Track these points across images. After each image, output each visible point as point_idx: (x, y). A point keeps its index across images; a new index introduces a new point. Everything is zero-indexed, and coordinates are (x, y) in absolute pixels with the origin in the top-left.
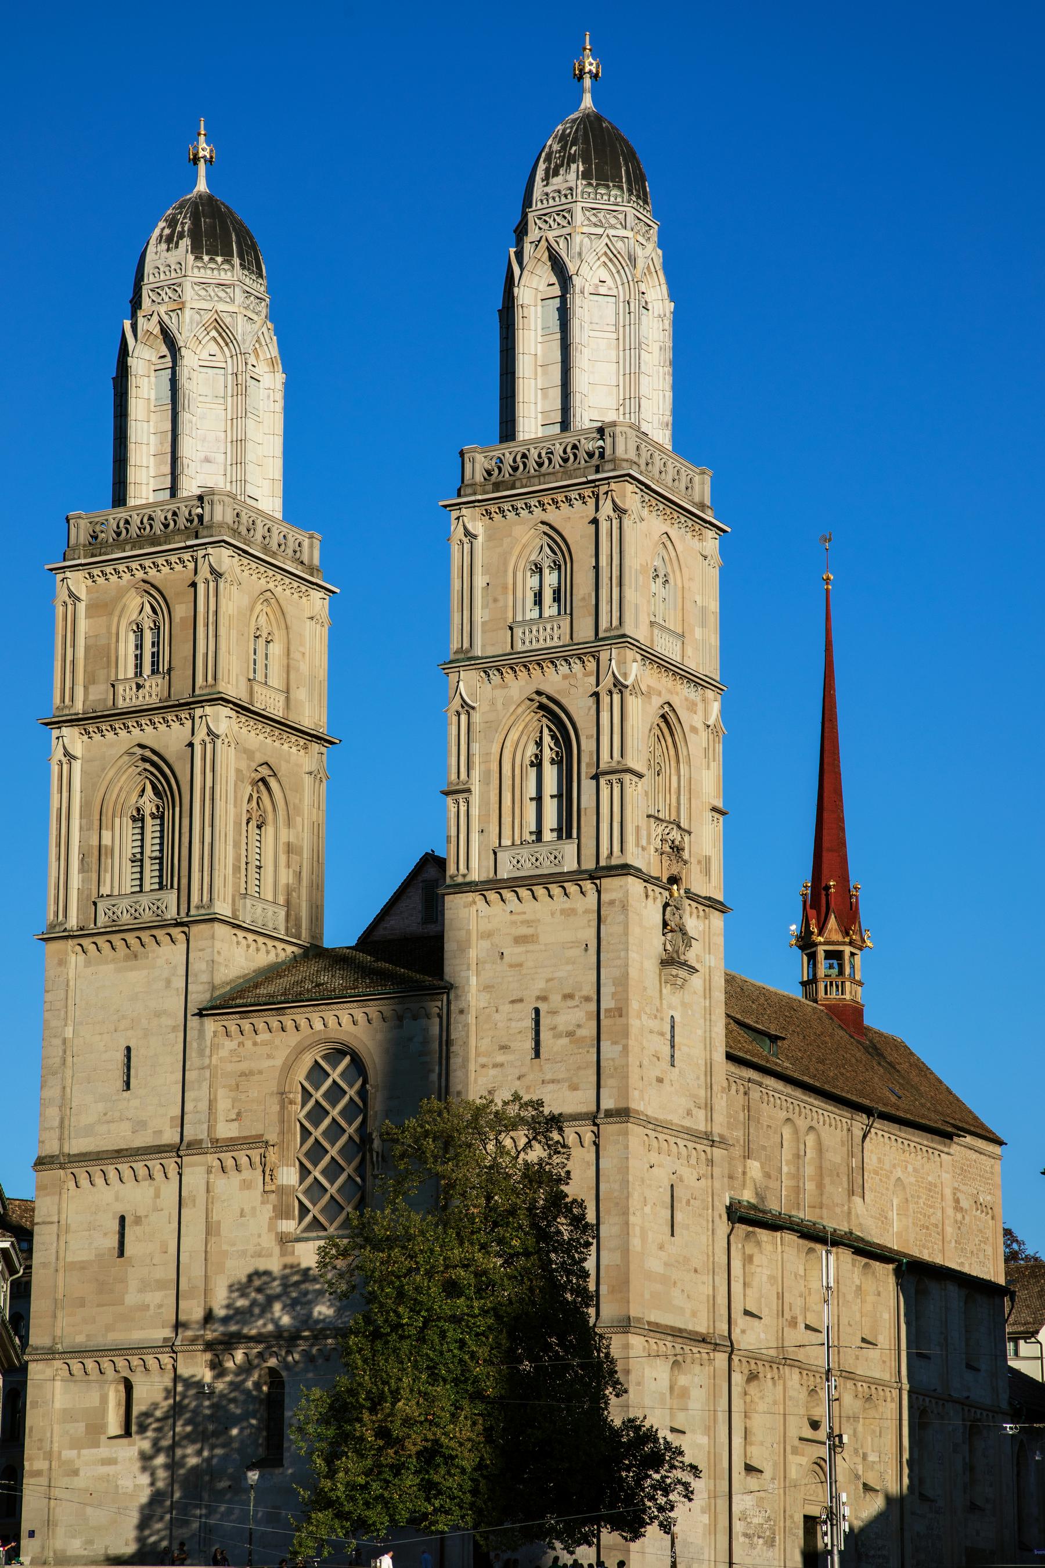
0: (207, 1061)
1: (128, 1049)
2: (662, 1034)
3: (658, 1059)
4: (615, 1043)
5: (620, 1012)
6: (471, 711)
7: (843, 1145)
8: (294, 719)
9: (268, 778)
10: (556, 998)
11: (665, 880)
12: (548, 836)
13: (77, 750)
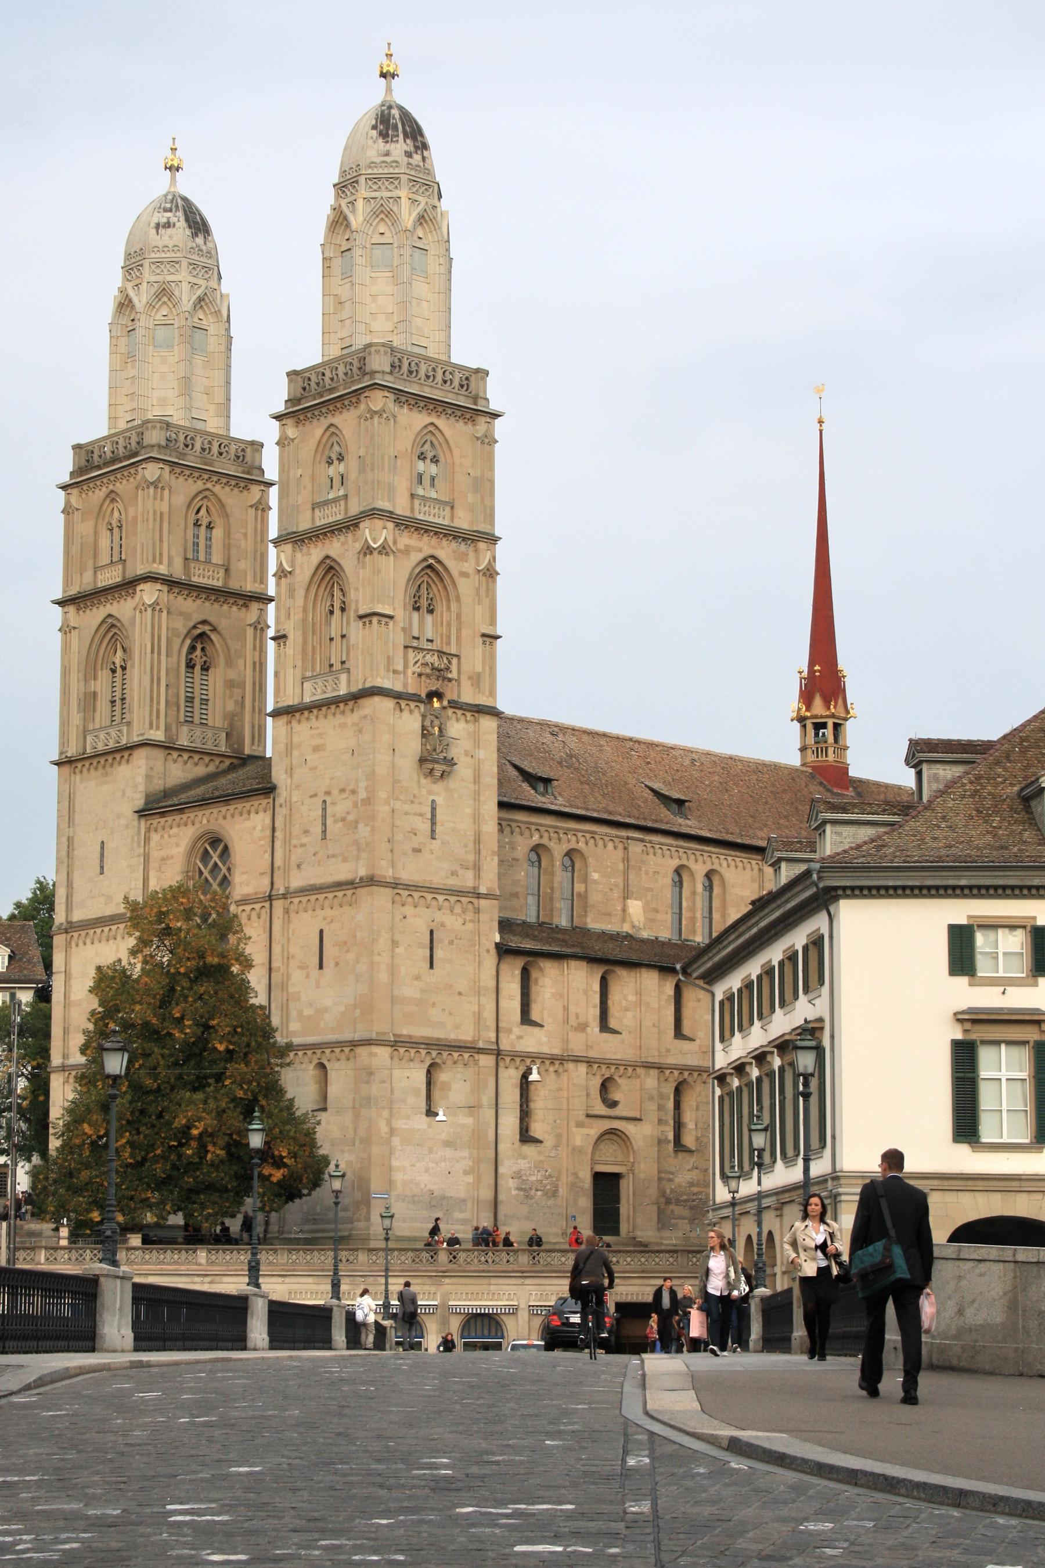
1: (103, 842)
2: (421, 815)
3: (415, 834)
4: (367, 825)
5: (368, 801)
7: (753, 880)
8: (234, 585)
9: (209, 633)
11: (423, 695)
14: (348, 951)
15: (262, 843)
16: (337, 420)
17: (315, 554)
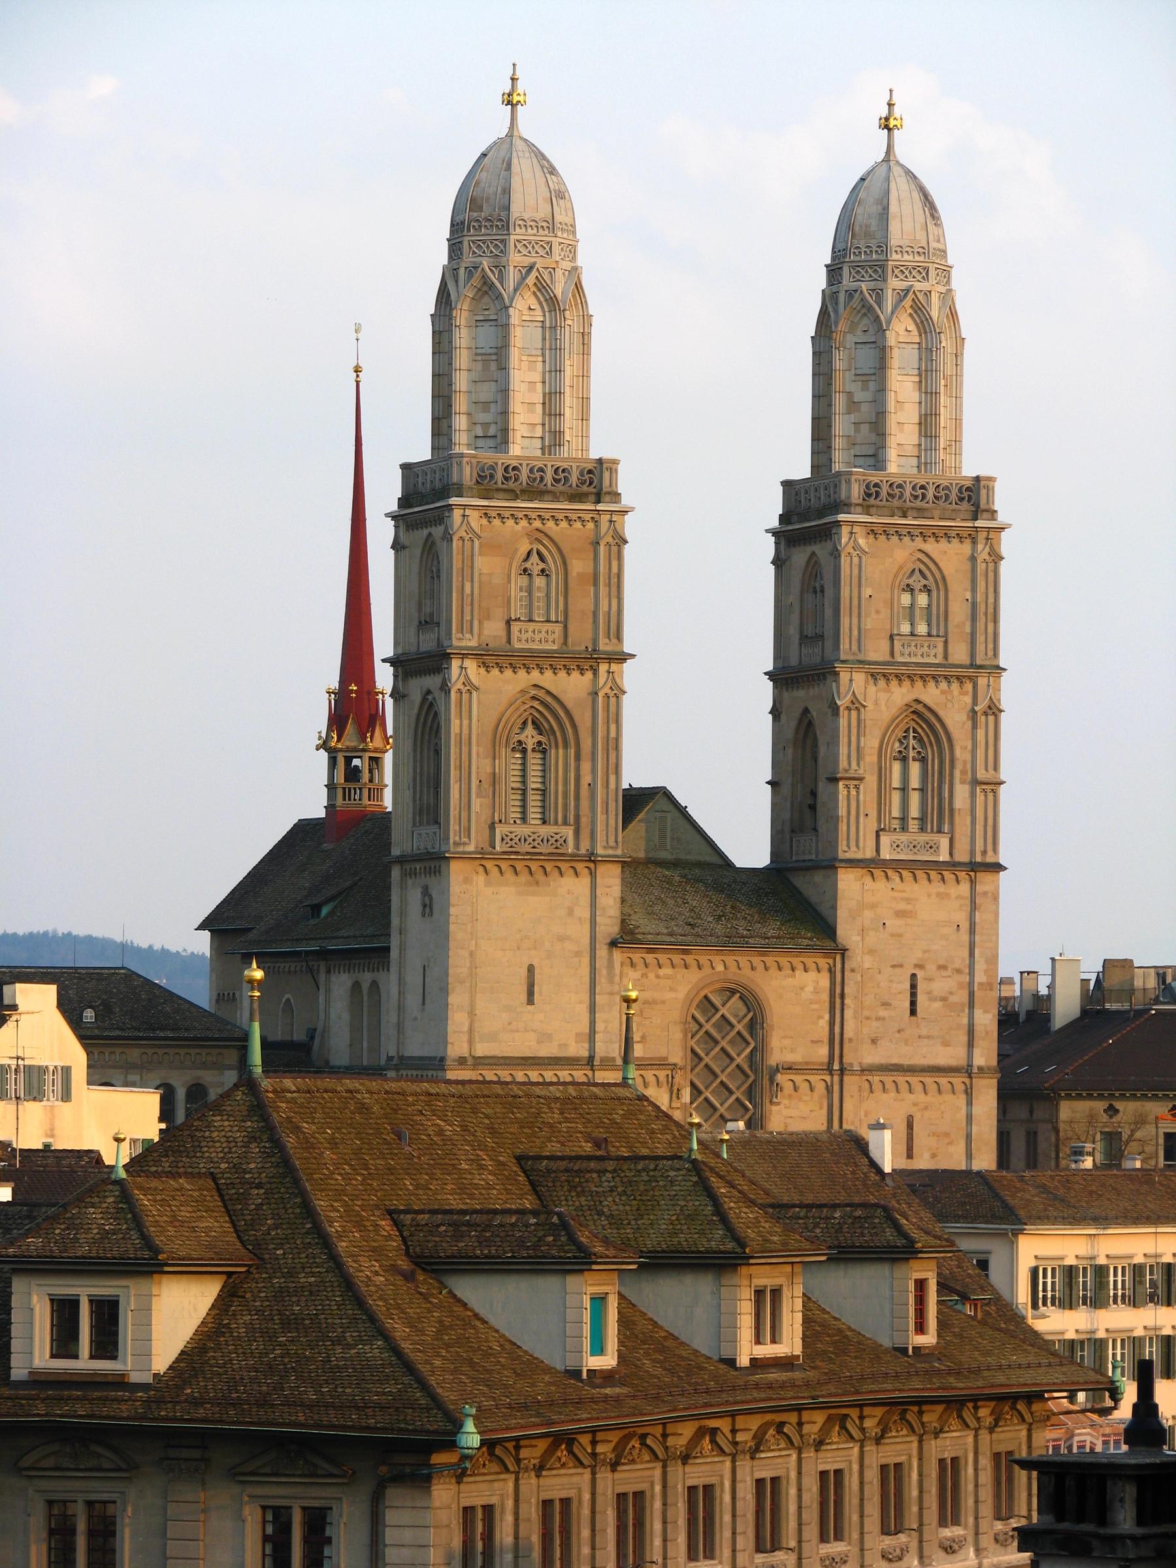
0: (616, 988)
1: (531, 969)
4: (986, 1012)
6: (862, 710)
10: (931, 968)
12: (913, 826)
13: (474, 679)
14: (950, 1143)
15: (814, 1006)
16: (930, 547)
17: (901, 694)
